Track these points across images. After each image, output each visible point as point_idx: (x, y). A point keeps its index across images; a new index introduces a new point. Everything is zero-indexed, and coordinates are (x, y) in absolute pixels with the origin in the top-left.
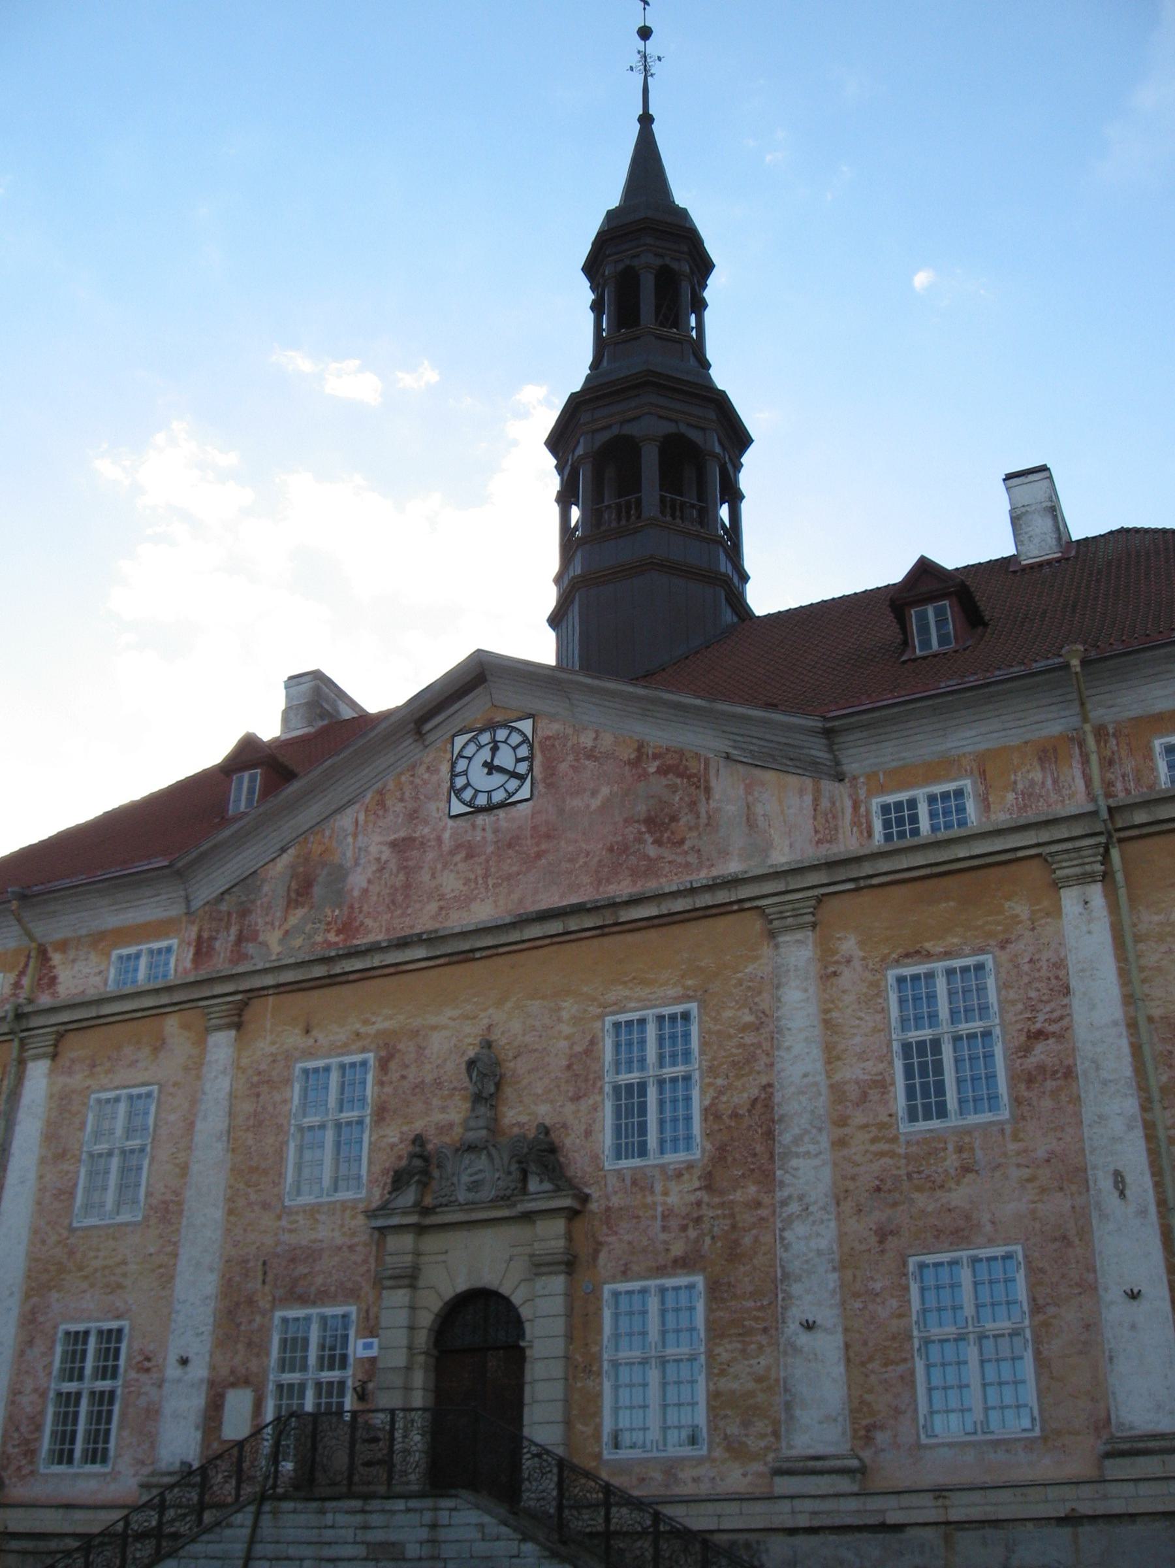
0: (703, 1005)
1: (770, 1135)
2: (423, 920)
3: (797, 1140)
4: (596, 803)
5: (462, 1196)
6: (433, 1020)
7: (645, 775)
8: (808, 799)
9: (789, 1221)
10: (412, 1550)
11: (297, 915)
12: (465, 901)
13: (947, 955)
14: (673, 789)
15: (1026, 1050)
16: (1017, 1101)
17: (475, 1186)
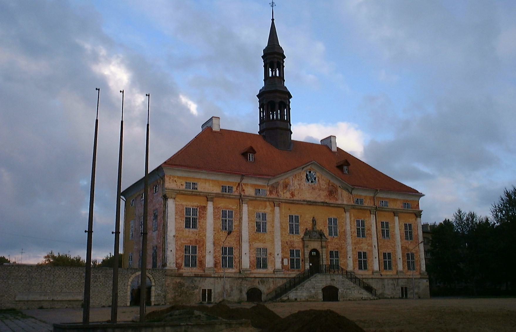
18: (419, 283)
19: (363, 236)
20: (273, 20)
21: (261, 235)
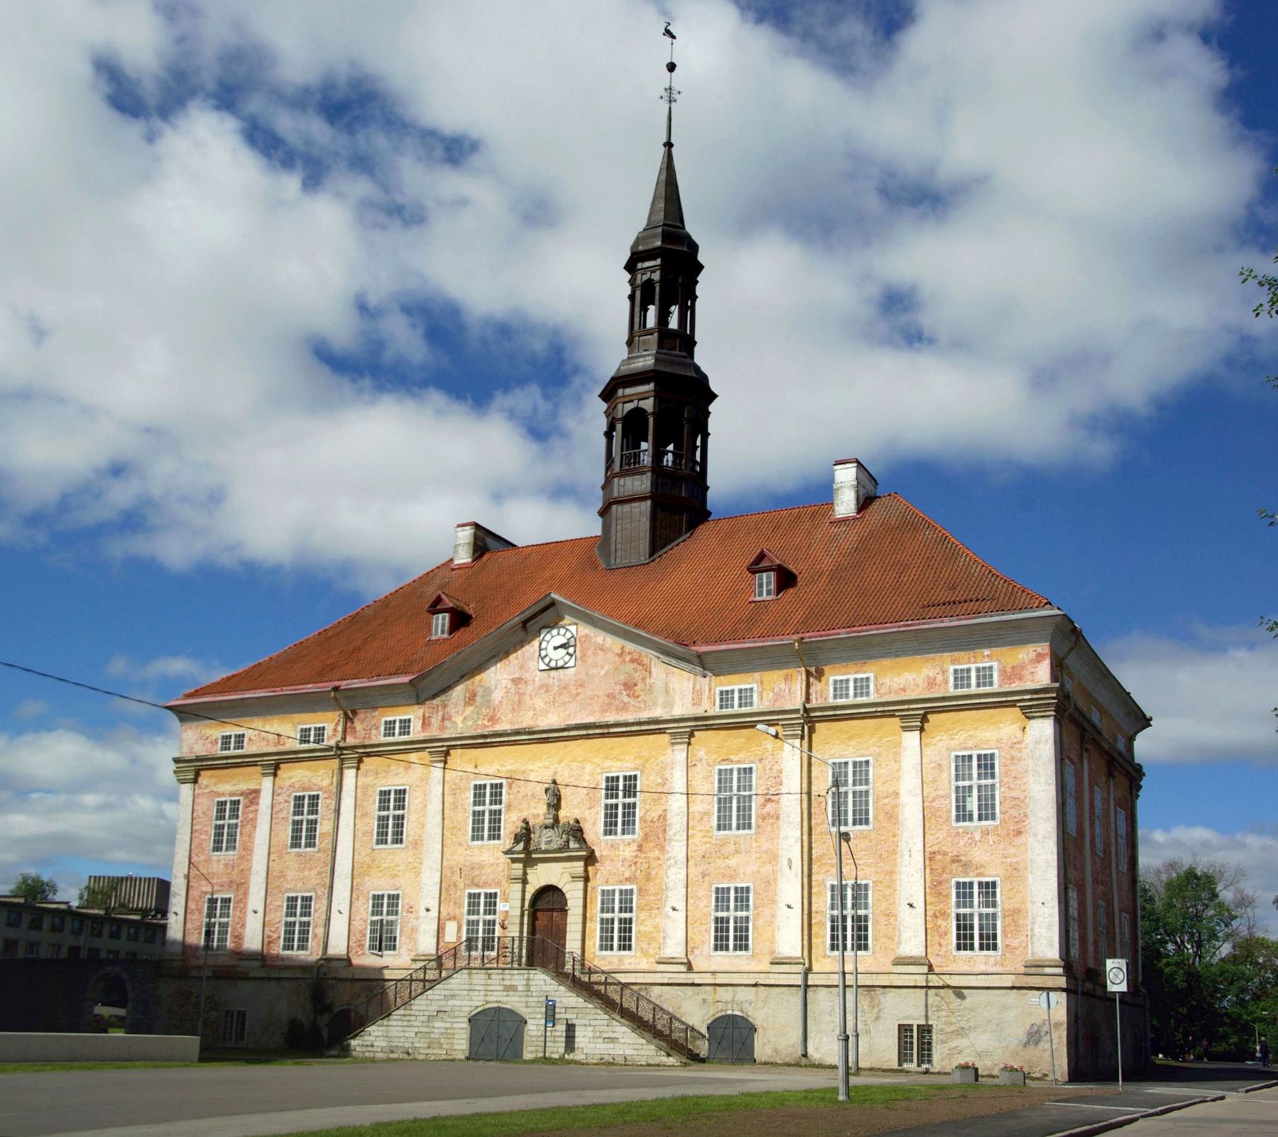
0: (642, 772)
1: (665, 831)
2: (526, 721)
3: (675, 834)
4: (603, 673)
5: (543, 847)
6: (531, 767)
7: (624, 662)
8: (691, 684)
9: (669, 867)
10: (520, 988)
11: (469, 710)
12: (545, 712)
13: (739, 762)
14: (636, 670)
15: (764, 806)
16: (758, 827)
17: (550, 842)
18: (1005, 1008)
19: (745, 824)
20: (669, 145)
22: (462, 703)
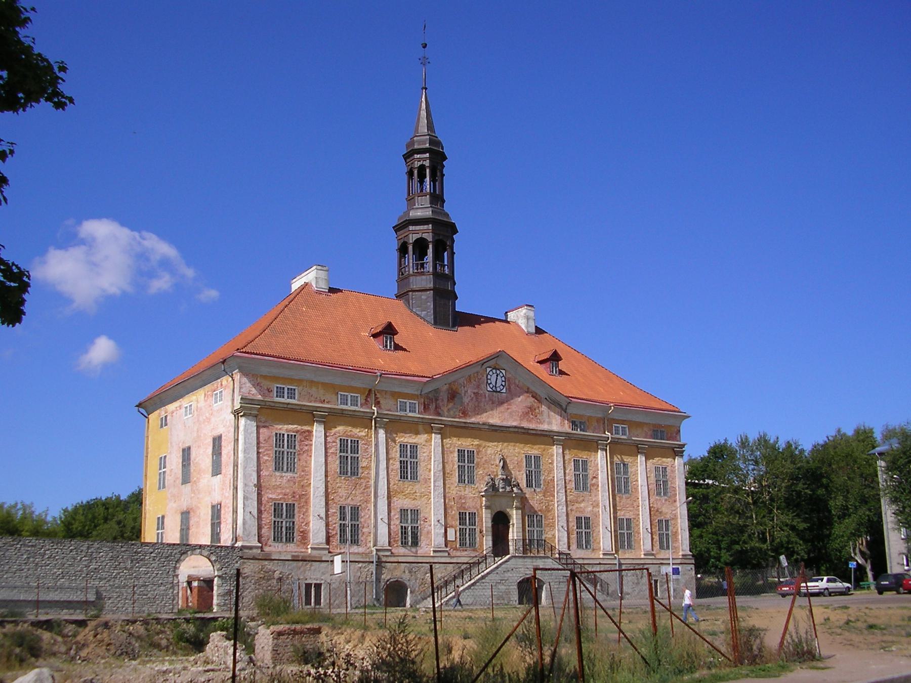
11: (451, 405)
19: (585, 488)
21: (408, 487)
22: (446, 401)
